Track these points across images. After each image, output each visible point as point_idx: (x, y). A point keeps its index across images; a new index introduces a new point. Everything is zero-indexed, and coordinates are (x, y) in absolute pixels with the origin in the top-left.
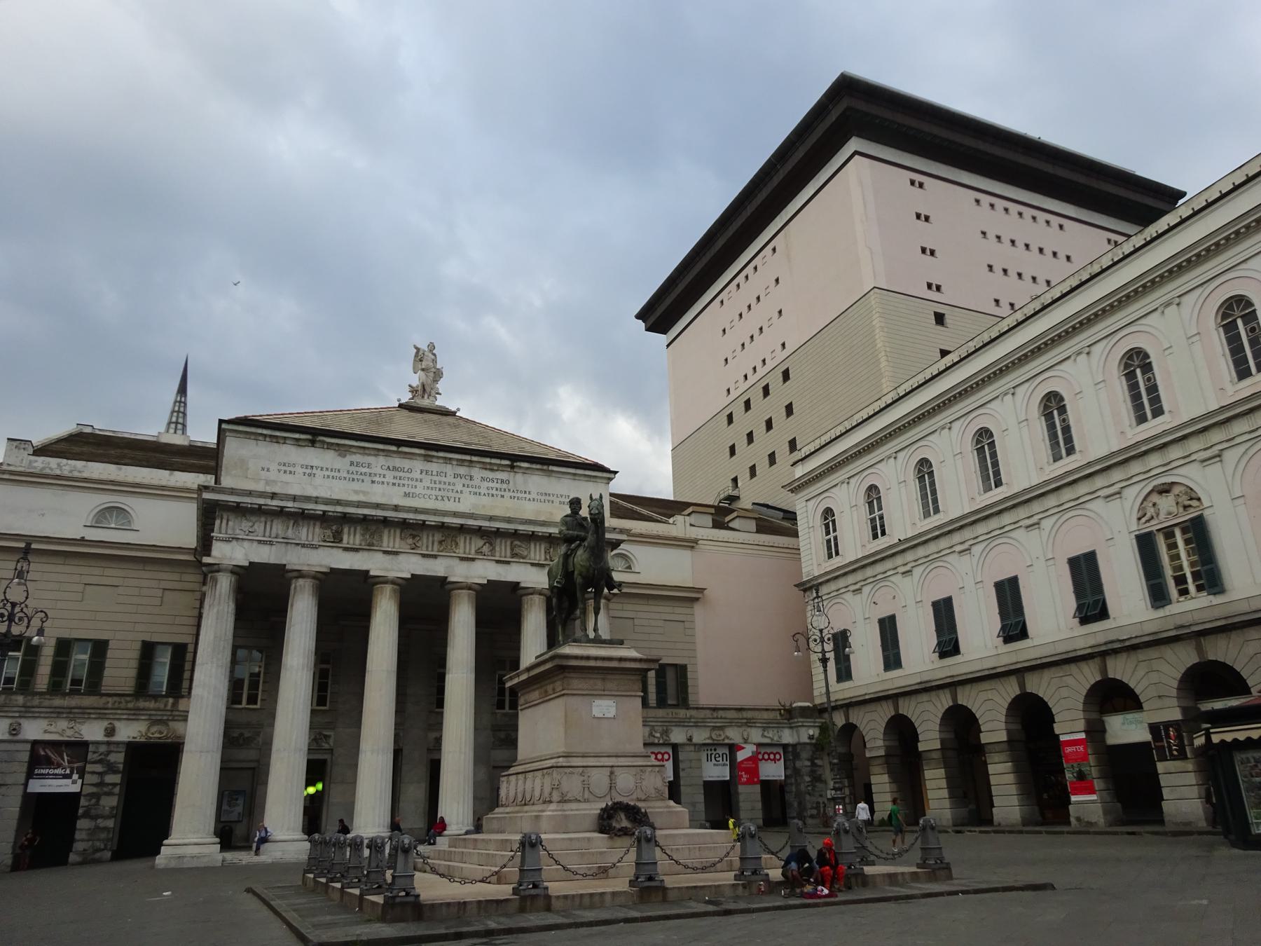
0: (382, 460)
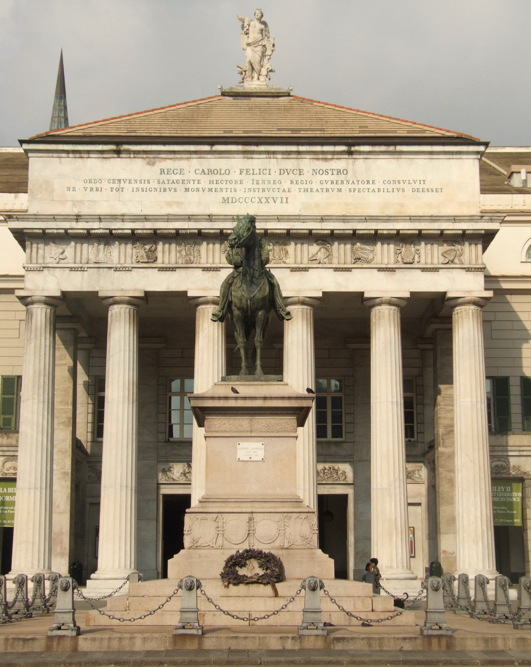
0: (195, 163)
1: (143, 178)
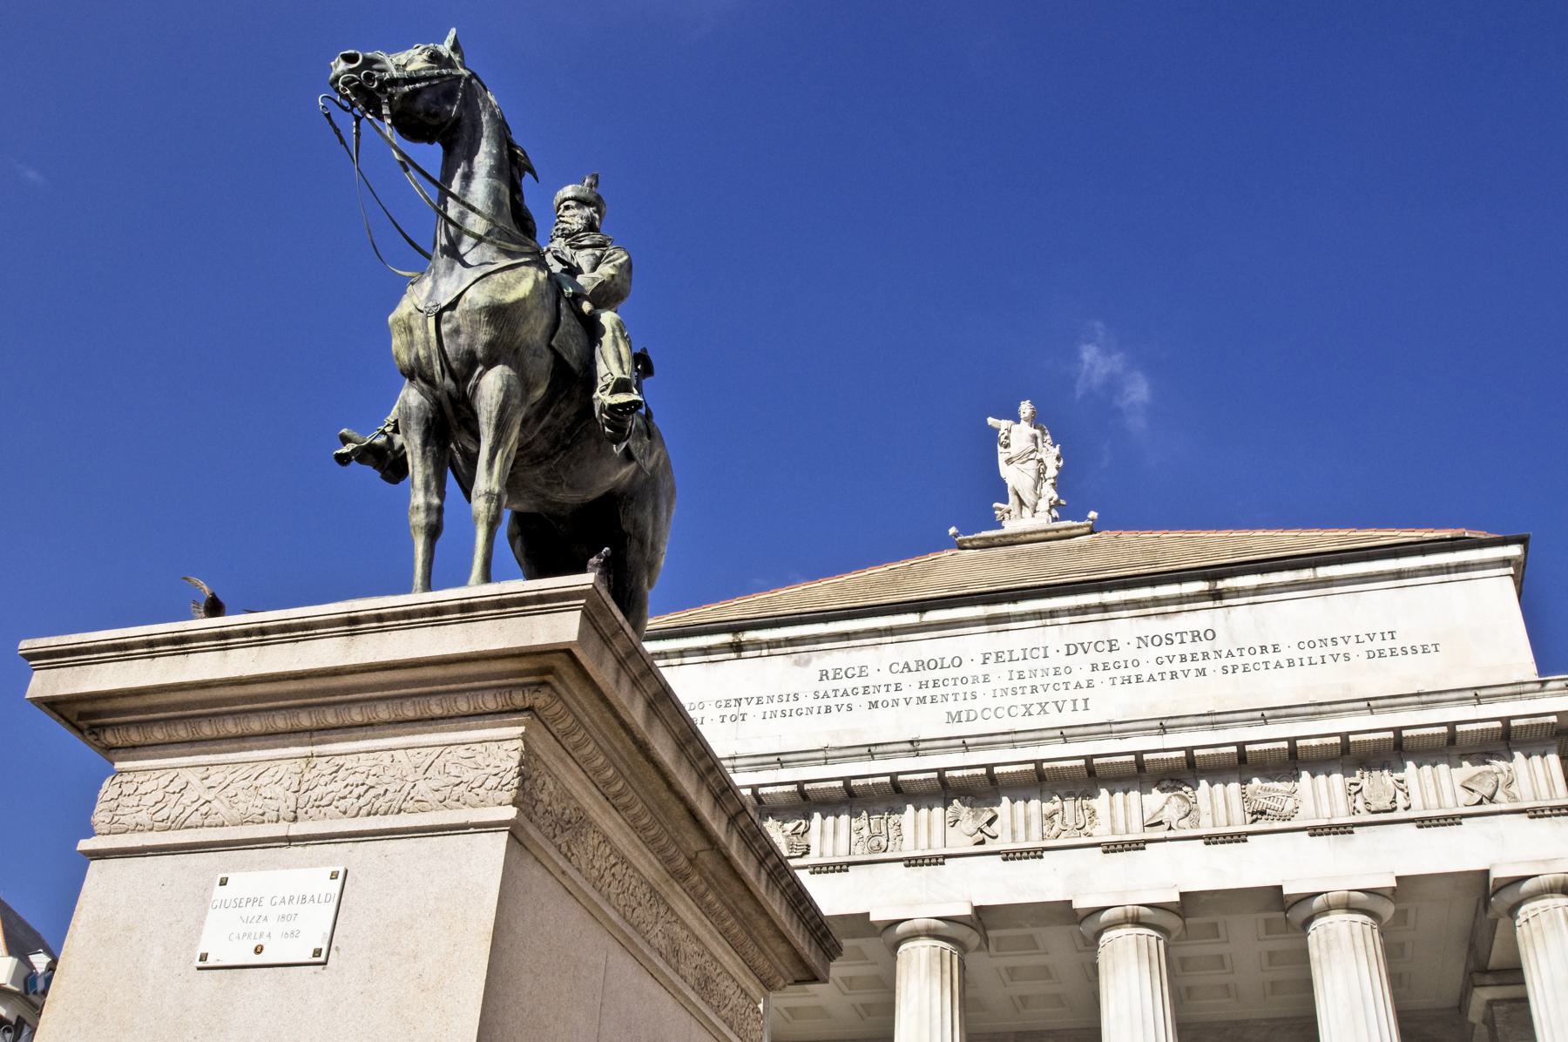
1: (784, 693)
